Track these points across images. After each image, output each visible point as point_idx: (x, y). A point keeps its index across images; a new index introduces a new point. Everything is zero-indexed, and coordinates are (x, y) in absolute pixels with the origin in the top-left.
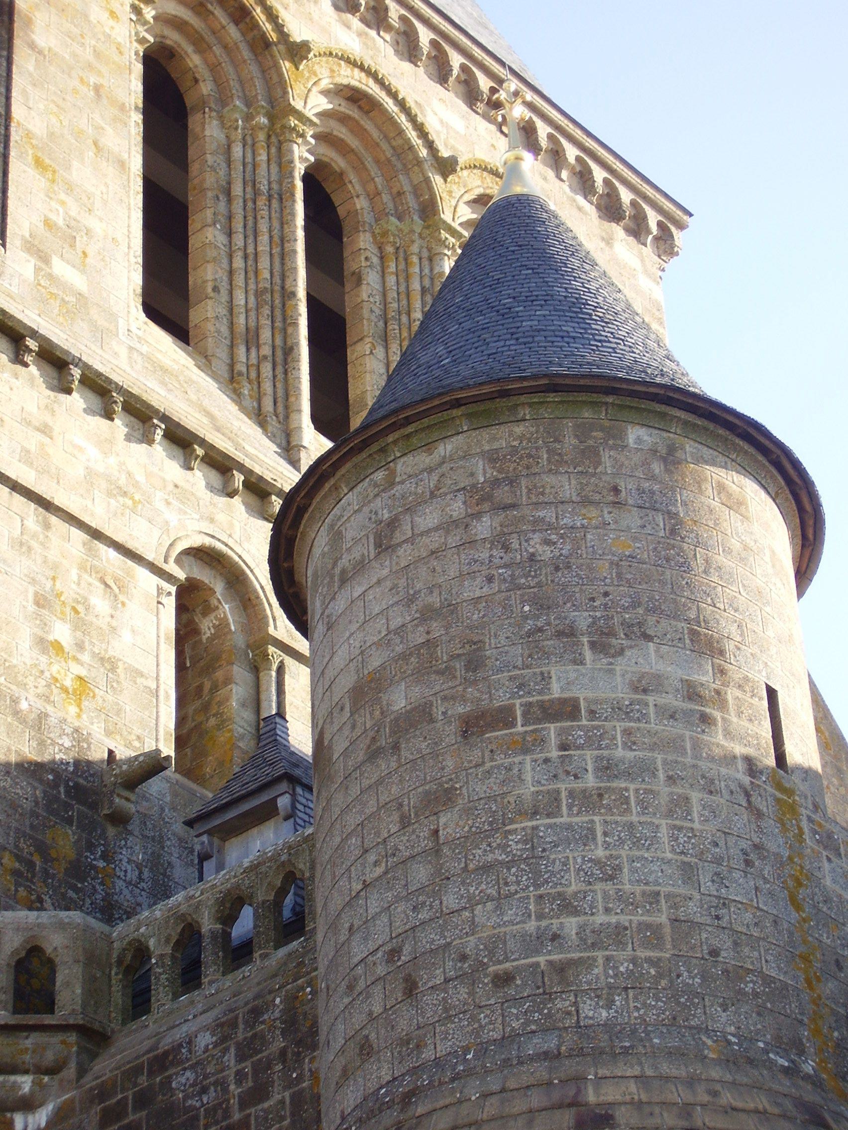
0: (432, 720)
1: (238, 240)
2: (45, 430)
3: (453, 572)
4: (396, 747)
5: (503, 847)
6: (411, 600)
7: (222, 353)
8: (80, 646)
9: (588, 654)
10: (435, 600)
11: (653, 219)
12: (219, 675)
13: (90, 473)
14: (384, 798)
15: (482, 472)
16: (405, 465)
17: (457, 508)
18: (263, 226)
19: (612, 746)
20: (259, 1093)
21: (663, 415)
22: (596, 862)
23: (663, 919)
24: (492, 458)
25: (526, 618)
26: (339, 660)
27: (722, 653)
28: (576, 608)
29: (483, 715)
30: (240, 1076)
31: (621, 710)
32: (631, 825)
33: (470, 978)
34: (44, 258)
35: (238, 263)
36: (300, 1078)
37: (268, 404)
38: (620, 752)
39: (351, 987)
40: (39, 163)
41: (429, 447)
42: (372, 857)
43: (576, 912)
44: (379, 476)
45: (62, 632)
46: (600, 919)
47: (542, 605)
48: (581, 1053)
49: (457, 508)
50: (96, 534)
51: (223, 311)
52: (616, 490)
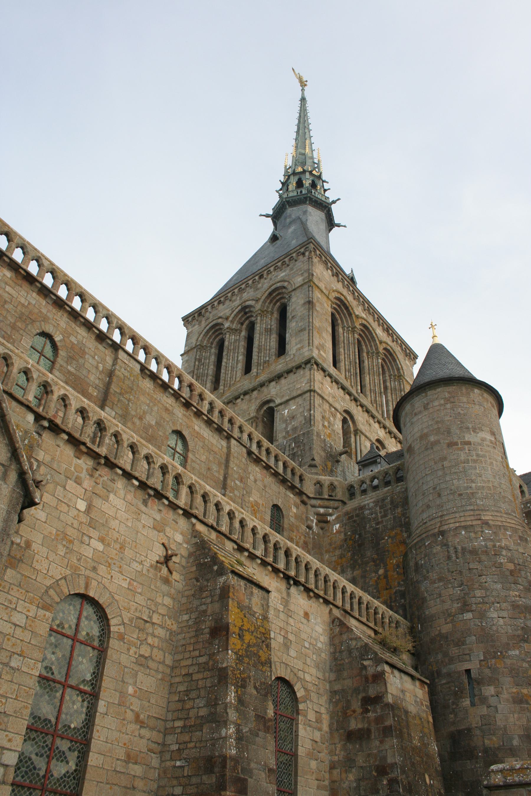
0: (440, 443)
1: (346, 352)
2: (322, 383)
3: (442, 414)
4: (432, 448)
5: (458, 469)
6: (433, 419)
7: (344, 373)
8: (329, 427)
9: (472, 433)
10: (439, 419)
11: (412, 356)
12: (348, 436)
13: (329, 393)
14: (430, 458)
15: (447, 395)
16: (429, 393)
17: (442, 402)
18: (351, 349)
19: (478, 451)
20: (385, 515)
21: (481, 388)
22: (477, 473)
23: (491, 485)
24: (449, 392)
25: (459, 424)
26: (416, 430)
27: (494, 435)
28: (469, 423)
29: (451, 443)
30: (380, 512)
31: (480, 444)
32: (483, 467)
33: (453, 494)
34: (319, 351)
35: (346, 356)
36: (395, 513)
37: (353, 384)
38: (480, 453)
39: (423, 495)
40: (318, 332)
41: (435, 389)
42: (428, 469)
43: (474, 483)
44: (424, 394)
45: (326, 424)
46: (479, 484)
47: (462, 422)
48: (479, 510)
49: (442, 402)
50: (331, 405)
51: (343, 365)
52: (474, 401)
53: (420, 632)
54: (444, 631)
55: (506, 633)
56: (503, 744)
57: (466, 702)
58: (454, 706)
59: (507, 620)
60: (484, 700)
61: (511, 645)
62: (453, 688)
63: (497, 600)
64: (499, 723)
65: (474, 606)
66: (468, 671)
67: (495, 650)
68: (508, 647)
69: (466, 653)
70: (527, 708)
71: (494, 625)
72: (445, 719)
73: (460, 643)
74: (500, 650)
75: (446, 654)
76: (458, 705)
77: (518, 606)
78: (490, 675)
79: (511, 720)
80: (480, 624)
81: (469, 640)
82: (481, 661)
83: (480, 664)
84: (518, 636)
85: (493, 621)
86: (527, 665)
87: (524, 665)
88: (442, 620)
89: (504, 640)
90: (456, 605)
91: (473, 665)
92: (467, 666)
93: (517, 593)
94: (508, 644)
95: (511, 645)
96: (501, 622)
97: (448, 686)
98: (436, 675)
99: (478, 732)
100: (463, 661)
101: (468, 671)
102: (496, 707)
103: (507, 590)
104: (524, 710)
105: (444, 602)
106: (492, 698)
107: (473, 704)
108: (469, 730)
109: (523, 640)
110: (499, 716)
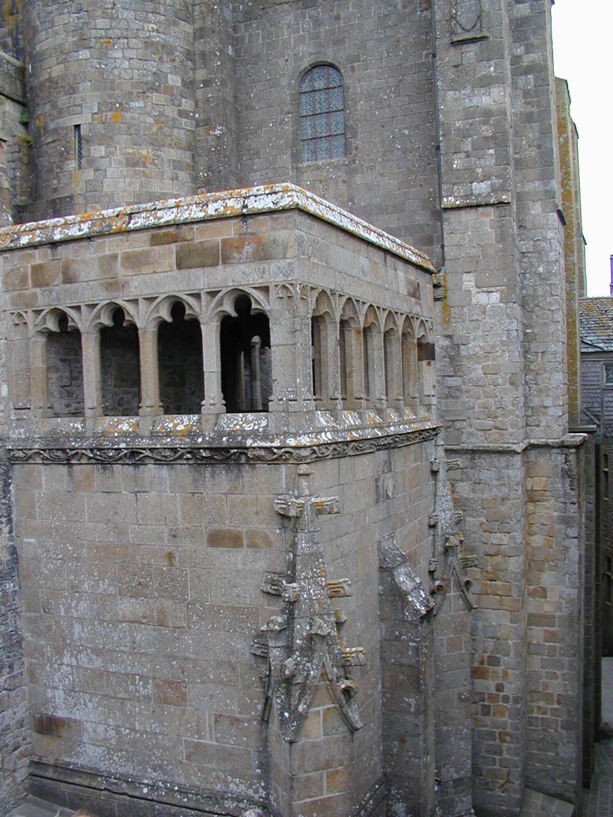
53: (31, 75)
54: (54, 75)
55: (132, 79)
57: (72, 165)
58: (58, 170)
59: (134, 62)
60: (92, 162)
61: (135, 95)
62: (59, 148)
63: (125, 33)
65: (93, 40)
66: (77, 127)
67: (114, 101)
70: (143, 172)
71: (116, 67)
73: (73, 90)
74: (120, 100)
75: (54, 106)
76: (62, 168)
77: (153, 44)
78: (103, 131)
79: (121, 185)
80: (98, 66)
81: (81, 87)
82: (95, 114)
83: (92, 117)
84: (146, 83)
85: (115, 62)
86: (152, 121)
87: (148, 121)
88: (53, 60)
89: (127, 88)
90: (71, 39)
91: (84, 119)
93: (155, 27)
94: (131, 93)
95: (135, 95)
96: (126, 64)
98: (42, 131)
99: (81, 200)
100: (73, 114)
101: (77, 127)
102: (105, 170)
103: (141, 21)
105: (57, 34)
107: (80, 167)
108: (71, 197)
109: (152, 89)
110: (107, 181)
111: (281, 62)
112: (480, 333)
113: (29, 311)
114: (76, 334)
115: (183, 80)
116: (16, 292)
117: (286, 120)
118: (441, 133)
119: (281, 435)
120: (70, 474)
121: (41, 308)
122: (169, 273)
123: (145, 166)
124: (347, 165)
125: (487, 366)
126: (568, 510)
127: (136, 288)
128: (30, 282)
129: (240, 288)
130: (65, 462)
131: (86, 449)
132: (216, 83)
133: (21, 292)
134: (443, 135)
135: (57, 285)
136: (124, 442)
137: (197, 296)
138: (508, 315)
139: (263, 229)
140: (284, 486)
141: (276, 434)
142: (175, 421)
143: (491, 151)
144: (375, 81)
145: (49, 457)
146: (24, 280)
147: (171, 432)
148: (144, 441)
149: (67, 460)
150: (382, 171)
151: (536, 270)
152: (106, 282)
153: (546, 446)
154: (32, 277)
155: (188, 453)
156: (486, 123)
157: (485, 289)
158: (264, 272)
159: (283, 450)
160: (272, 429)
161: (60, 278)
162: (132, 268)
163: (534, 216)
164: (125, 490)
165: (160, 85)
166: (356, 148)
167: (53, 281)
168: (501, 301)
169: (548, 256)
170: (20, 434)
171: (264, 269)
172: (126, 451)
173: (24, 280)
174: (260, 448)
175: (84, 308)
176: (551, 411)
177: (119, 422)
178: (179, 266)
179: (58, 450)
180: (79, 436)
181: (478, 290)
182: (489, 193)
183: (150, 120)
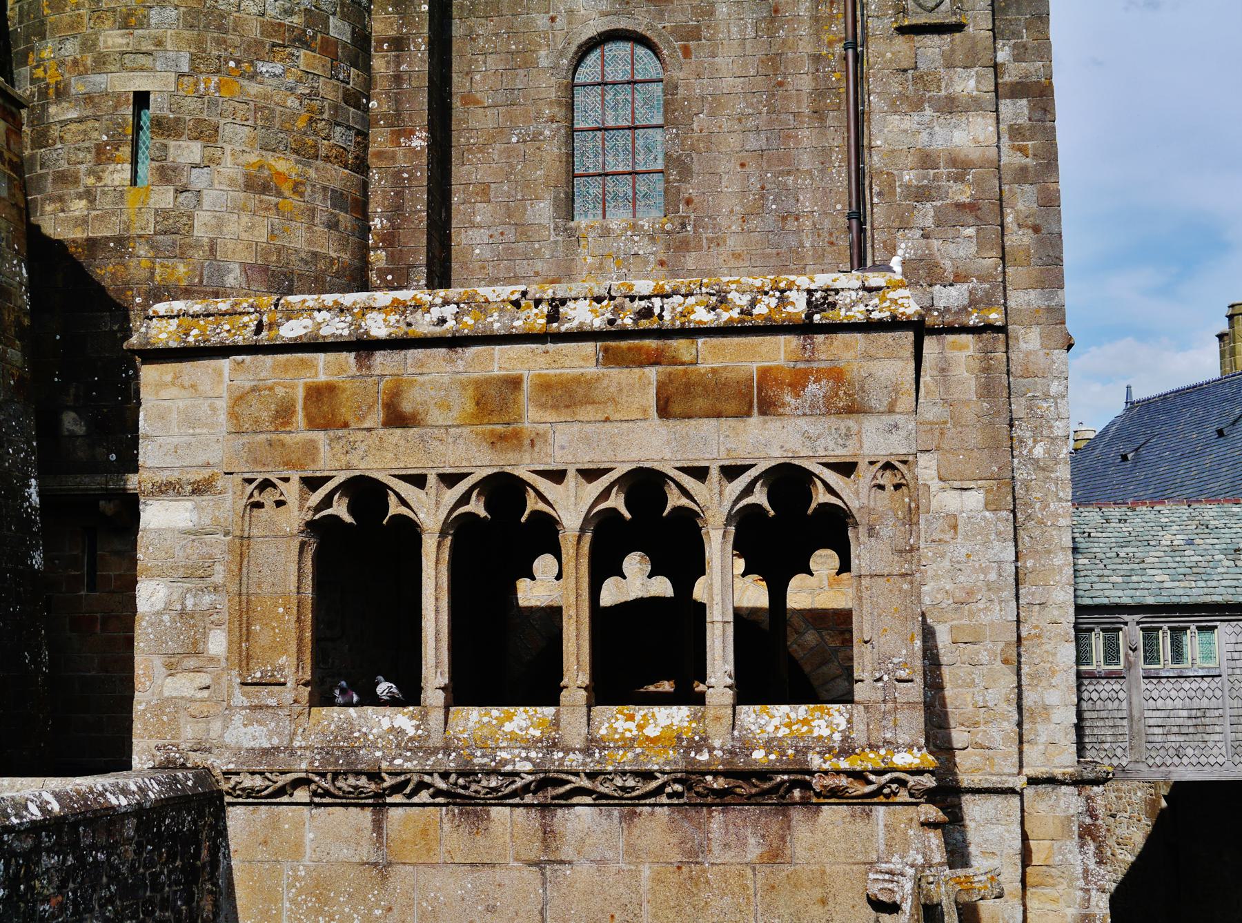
56: (201, 281)
64: (198, 232)
68: (255, 51)
69: (144, 49)
72: (63, 211)
74: (237, 54)
75: (88, 45)
76: (99, 179)
81: (155, 16)
82: (183, 75)
84: (291, 29)
92: (140, 83)
97: (82, 127)
98: (51, 91)
99: (142, 250)
100: (133, 70)
101: (141, 99)
104: (268, 209)
106: (195, 171)
108: (121, 241)
109: (299, 40)
111: (542, 21)
112: (946, 563)
113: (295, 477)
114: (409, 531)
115: (353, 32)
116: (263, 437)
117: (547, 133)
118: (876, 189)
119: (878, 747)
120: (378, 826)
121: (326, 474)
122: (640, 424)
123: (279, 194)
124: (668, 233)
125: (958, 627)
126: (1093, 903)
127: (562, 448)
128: (300, 418)
129: (796, 462)
130: (371, 801)
131: (431, 774)
132: (417, 46)
133: (274, 436)
134: (880, 194)
135: (369, 430)
136: (523, 759)
137: (700, 473)
138: (998, 534)
139: (849, 355)
140: (882, 847)
141: (871, 747)
142: (638, 717)
143: (970, 231)
144: (731, 81)
145: (332, 789)
146: (284, 414)
147: (633, 739)
148: (571, 756)
149: (376, 795)
150: (739, 250)
151: (1030, 451)
152: (492, 431)
153: (1052, 781)
154: (305, 408)
155: (676, 781)
156: (959, 178)
157: (957, 484)
158: (847, 436)
159: (888, 776)
160: (859, 736)
161: (376, 417)
162: (555, 407)
163: (1027, 354)
164: (516, 860)
165: (314, 37)
166: (688, 202)
167: (362, 418)
168: (986, 506)
169: (1051, 427)
170: (254, 738)
171: (849, 429)
172: (530, 778)
173: (284, 414)
174: (838, 772)
175: (432, 480)
176: (1056, 716)
177: (510, 718)
178: (664, 411)
179: (358, 774)
180: (419, 747)
181: (942, 484)
182: (965, 308)
183: (292, 102)
